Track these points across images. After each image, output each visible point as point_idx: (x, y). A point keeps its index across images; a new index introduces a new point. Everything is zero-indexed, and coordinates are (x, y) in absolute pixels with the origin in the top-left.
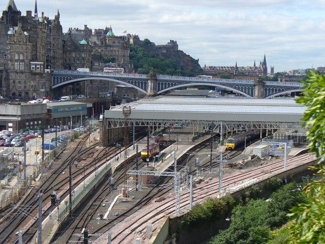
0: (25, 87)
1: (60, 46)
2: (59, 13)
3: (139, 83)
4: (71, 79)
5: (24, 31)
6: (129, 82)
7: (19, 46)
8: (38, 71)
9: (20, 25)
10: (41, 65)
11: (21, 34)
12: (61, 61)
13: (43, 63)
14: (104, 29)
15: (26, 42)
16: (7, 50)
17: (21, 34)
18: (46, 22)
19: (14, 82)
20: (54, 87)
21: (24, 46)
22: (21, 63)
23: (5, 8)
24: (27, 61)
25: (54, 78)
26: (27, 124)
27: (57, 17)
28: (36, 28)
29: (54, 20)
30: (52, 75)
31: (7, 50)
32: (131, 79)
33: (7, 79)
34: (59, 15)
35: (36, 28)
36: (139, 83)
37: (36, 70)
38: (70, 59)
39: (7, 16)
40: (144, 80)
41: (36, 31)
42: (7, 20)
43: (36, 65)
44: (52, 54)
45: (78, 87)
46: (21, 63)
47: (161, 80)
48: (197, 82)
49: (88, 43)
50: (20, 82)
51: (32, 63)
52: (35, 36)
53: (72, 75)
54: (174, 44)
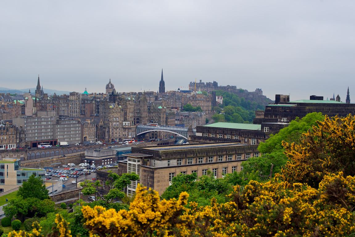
0: (119, 136)
3: (183, 133)
8: (127, 127)
14: (213, 83)
15: (120, 111)
19: (113, 133)
20: (137, 135)
21: (119, 114)
24: (121, 122)
26: (103, 161)
28: (126, 103)
30: (137, 128)
31: (109, 116)
32: (179, 131)
33: (109, 132)
35: (126, 103)
36: (183, 133)
40: (186, 131)
50: (116, 133)
54: (259, 91)
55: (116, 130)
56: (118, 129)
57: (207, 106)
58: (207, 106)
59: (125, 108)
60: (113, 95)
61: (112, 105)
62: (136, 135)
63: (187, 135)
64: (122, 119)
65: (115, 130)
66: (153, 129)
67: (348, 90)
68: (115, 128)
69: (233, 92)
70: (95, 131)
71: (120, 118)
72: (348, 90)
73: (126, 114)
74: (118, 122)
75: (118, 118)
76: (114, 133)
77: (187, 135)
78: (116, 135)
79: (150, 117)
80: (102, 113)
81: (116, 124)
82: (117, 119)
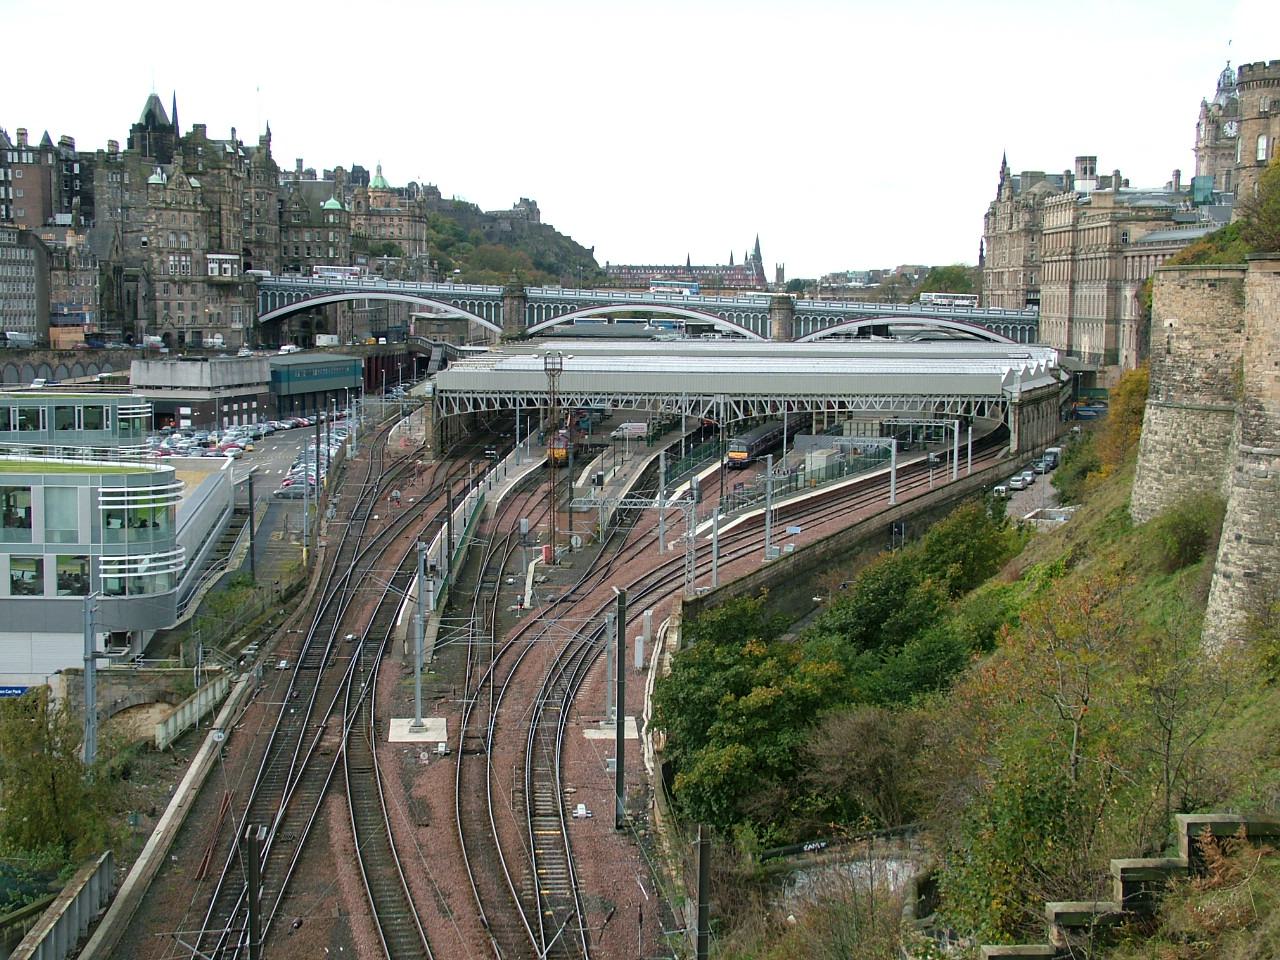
1: (273, 215)
2: (268, 129)
3: (480, 306)
4: (307, 298)
5: (189, 174)
6: (455, 305)
7: (176, 213)
9: (178, 160)
10: (232, 262)
11: (181, 183)
12: (275, 253)
13: (237, 257)
14: (350, 170)
16: (149, 225)
17: (181, 183)
18: (241, 153)
19: (167, 306)
22: (183, 258)
23: (137, 116)
24: (197, 253)
25: (265, 295)
26: (226, 408)
27: (266, 140)
29: (258, 149)
30: (259, 287)
31: (149, 225)
32: (461, 296)
33: (150, 298)
34: (269, 133)
36: (480, 306)
37: (220, 275)
38: (297, 248)
39: (143, 138)
40: (493, 298)
41: (218, 176)
42: (144, 147)
43: (221, 262)
44: (253, 234)
45: (320, 317)
46: (183, 258)
47: (536, 300)
48: (628, 303)
49: (343, 206)
50: (180, 307)
51: (209, 256)
52: (216, 188)
53: (310, 288)
54: (530, 208)
55: (180, 292)
56: (189, 288)
57: (415, 240)
58: (415, 240)
59: (213, 192)
60: (155, 129)
61: (159, 170)
62: (256, 318)
63: (497, 316)
64: (204, 244)
65: (174, 289)
66: (336, 294)
67: (1004, 163)
68: (175, 283)
69: (436, 208)
70: (98, 291)
71: (193, 234)
72: (1004, 163)
73: (220, 220)
74: (188, 252)
75: (186, 234)
76: (174, 304)
77: (497, 316)
78: (179, 313)
79: (285, 248)
80: (112, 209)
81: (180, 261)
82: (184, 238)
